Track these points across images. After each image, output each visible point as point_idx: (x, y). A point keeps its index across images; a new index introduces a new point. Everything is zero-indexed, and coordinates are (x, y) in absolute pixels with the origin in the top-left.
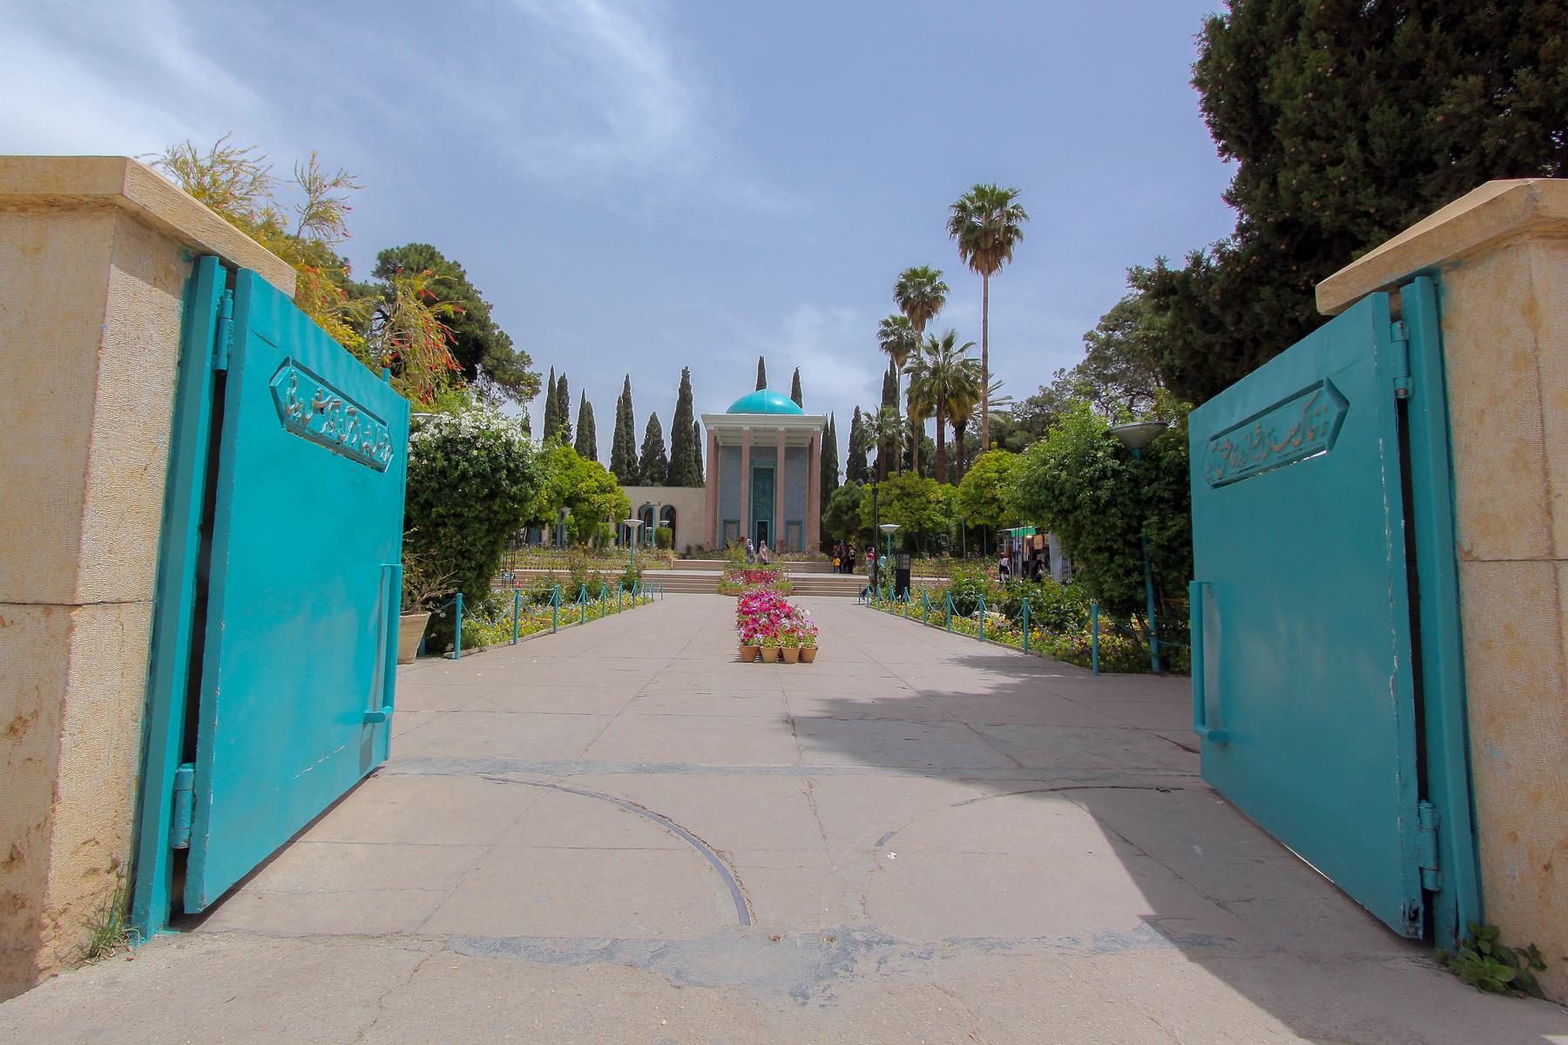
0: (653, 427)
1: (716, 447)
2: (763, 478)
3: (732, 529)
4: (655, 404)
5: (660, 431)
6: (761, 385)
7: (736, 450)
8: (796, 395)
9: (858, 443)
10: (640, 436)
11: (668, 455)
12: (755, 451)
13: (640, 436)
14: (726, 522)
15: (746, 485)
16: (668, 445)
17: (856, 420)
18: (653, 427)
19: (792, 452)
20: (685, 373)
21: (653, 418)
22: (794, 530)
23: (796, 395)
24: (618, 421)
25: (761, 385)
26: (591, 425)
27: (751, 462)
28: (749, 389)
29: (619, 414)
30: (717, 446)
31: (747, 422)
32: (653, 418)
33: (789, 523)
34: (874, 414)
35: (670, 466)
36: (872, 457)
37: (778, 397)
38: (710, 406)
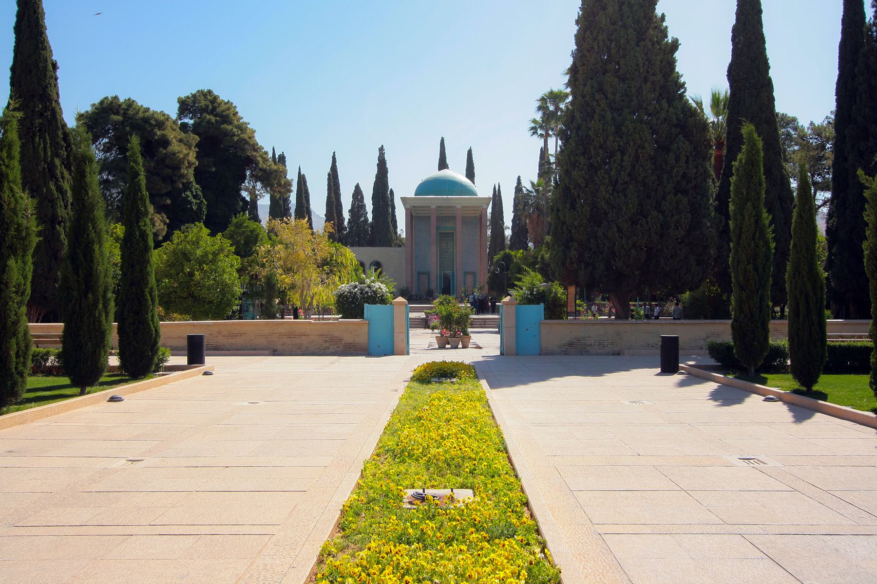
0: (358, 193)
1: (412, 217)
4: (358, 177)
5: (362, 197)
6: (443, 164)
10: (347, 202)
11: (370, 217)
13: (347, 202)
14: (419, 273)
17: (519, 189)
18: (358, 193)
20: (381, 149)
21: (357, 187)
24: (329, 189)
25: (443, 164)
27: (438, 228)
29: (329, 185)
30: (412, 216)
32: (357, 187)
35: (372, 225)
38: (403, 187)
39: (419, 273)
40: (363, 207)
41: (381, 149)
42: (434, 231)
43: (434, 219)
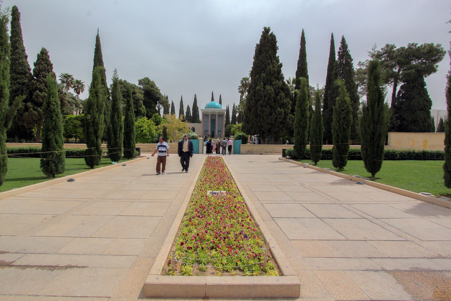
0: (188, 108)
2: (213, 121)
3: (207, 132)
4: (188, 103)
6: (213, 100)
7: (208, 115)
8: (220, 102)
9: (234, 112)
11: (192, 115)
12: (212, 115)
14: (205, 131)
15: (210, 124)
16: (191, 112)
17: (234, 107)
19: (219, 115)
20: (195, 95)
21: (188, 106)
22: (220, 133)
23: (220, 102)
26: (174, 108)
28: (209, 101)
31: (210, 110)
32: (188, 106)
33: (218, 131)
34: (237, 105)
36: (237, 115)
37: (216, 103)
38: (201, 107)
39: (205, 131)
40: (190, 112)
41: (195, 95)
42: (210, 119)
43: (210, 116)
